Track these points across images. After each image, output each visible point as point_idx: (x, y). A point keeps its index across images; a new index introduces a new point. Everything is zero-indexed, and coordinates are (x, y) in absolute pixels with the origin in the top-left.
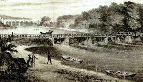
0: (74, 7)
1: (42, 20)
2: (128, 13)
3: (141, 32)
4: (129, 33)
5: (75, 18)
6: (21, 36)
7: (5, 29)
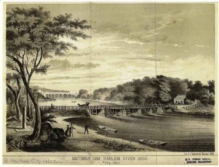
0: (110, 81)
1: (80, 93)
2: (159, 87)
3: (172, 103)
4: (160, 105)
5: (110, 91)
6: (60, 107)
7: (46, 101)
